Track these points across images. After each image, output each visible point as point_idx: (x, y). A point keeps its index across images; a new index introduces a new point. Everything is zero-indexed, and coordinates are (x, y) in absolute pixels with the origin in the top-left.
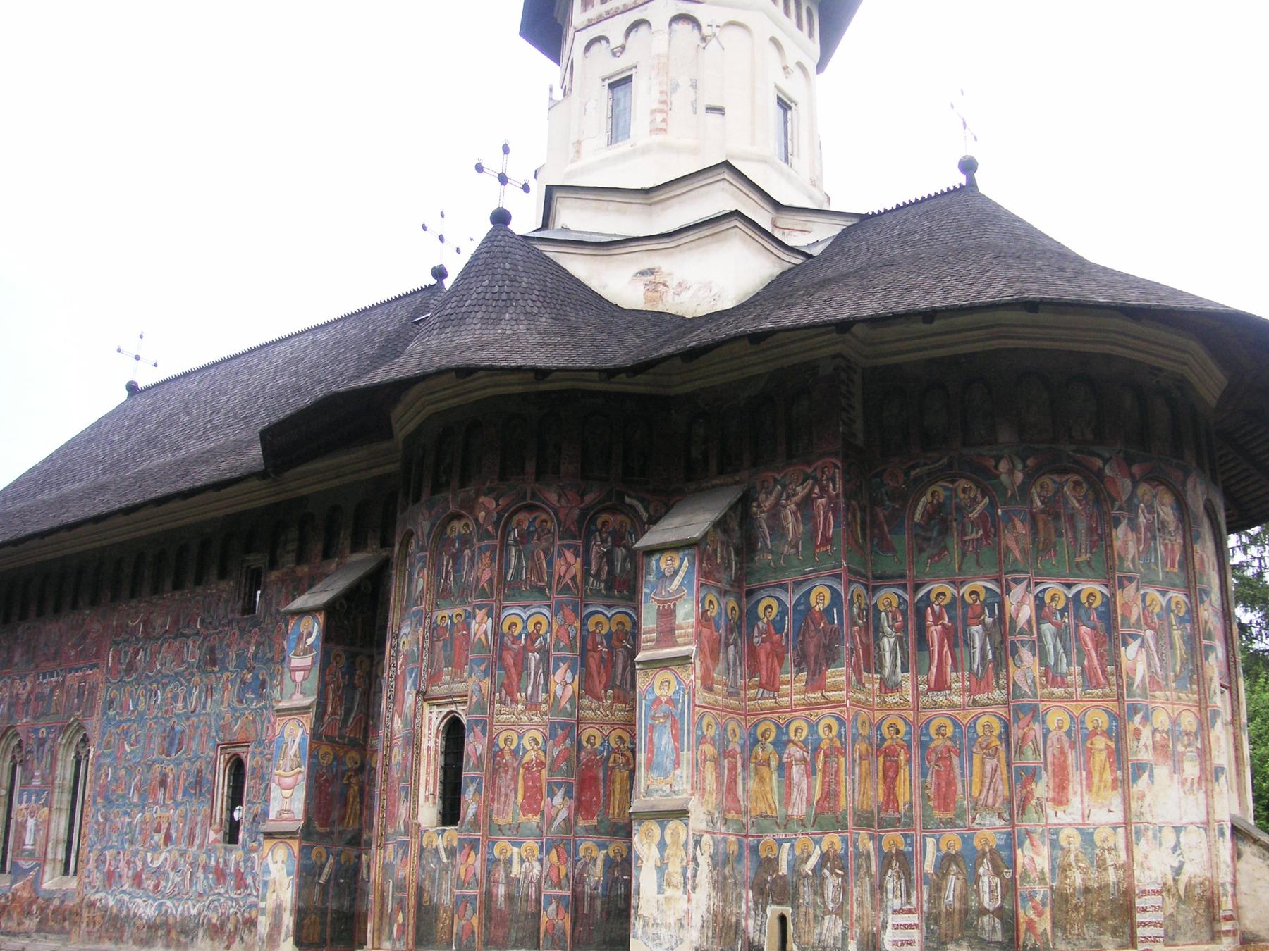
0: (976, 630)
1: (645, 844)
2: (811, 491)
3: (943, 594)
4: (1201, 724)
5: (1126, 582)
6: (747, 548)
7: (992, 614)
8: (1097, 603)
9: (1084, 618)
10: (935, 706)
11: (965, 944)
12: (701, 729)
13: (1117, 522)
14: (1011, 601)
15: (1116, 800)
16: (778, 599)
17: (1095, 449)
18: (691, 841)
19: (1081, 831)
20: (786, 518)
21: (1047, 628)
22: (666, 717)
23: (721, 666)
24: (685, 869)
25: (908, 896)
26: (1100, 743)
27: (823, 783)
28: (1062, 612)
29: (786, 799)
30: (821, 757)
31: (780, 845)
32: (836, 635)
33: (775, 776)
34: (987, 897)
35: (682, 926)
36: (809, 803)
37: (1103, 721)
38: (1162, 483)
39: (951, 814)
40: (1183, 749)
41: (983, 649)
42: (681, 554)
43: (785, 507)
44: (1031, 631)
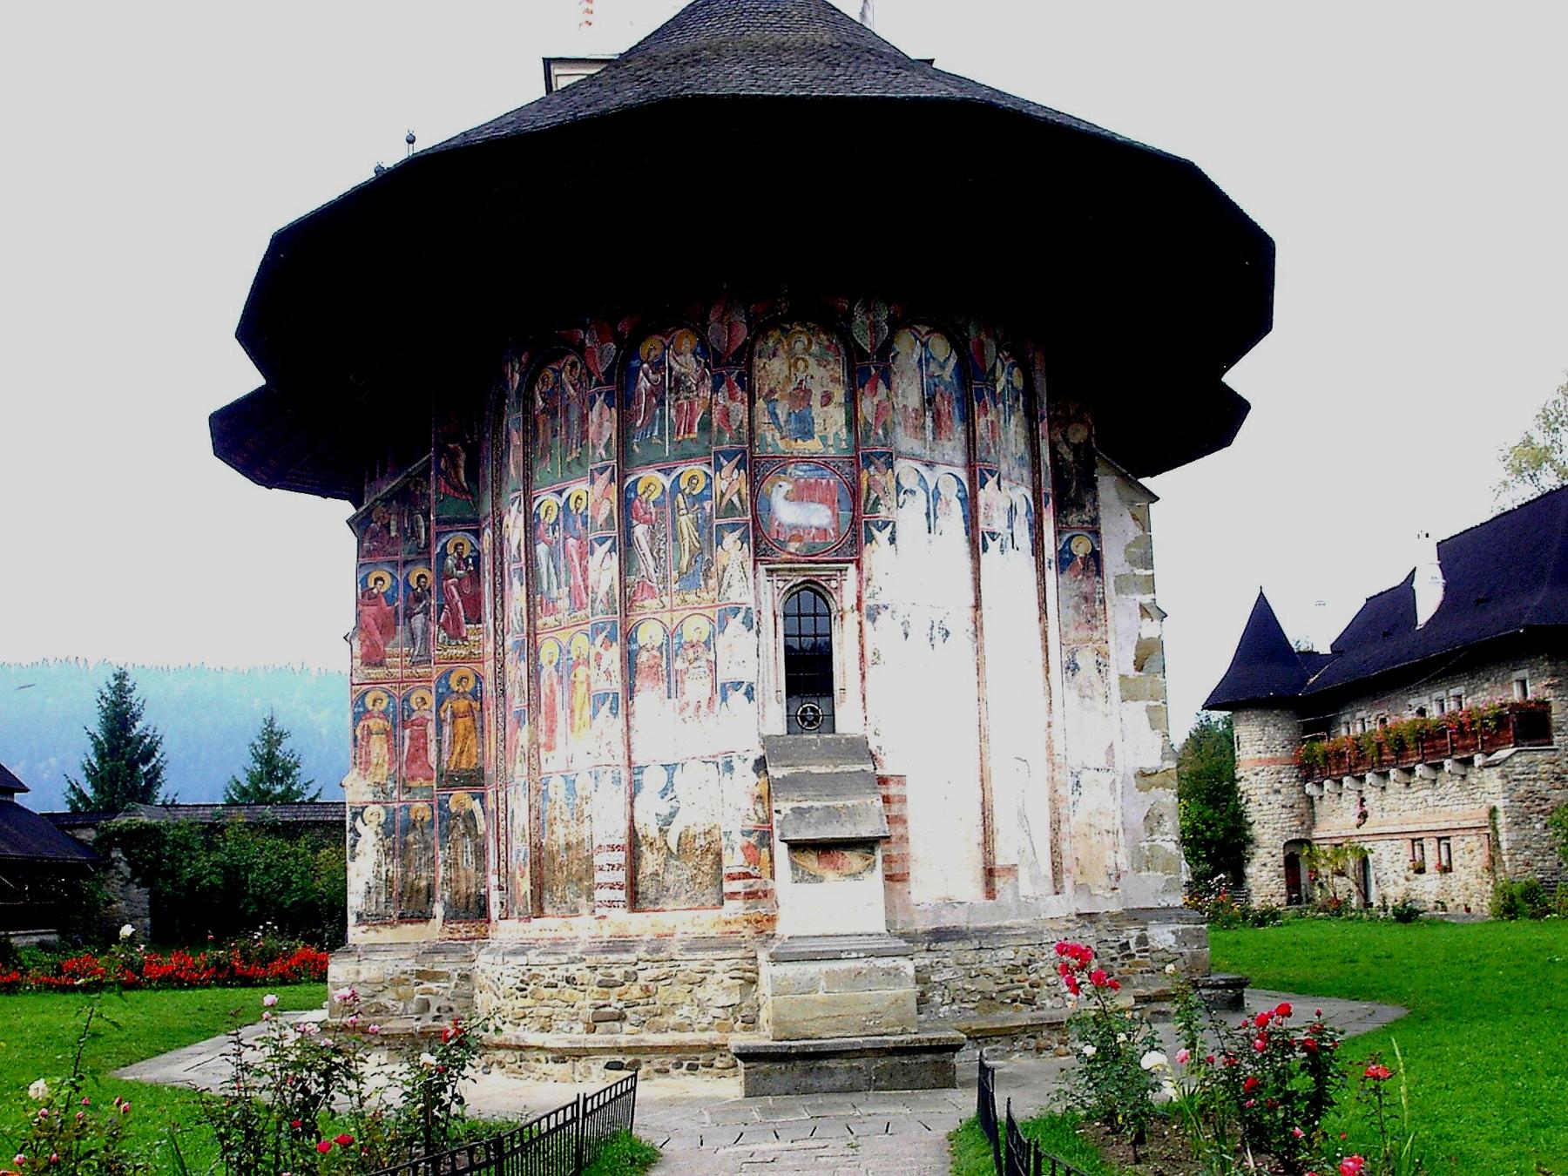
12: (363, 703)
13: (593, 401)
23: (401, 634)
26: (581, 671)
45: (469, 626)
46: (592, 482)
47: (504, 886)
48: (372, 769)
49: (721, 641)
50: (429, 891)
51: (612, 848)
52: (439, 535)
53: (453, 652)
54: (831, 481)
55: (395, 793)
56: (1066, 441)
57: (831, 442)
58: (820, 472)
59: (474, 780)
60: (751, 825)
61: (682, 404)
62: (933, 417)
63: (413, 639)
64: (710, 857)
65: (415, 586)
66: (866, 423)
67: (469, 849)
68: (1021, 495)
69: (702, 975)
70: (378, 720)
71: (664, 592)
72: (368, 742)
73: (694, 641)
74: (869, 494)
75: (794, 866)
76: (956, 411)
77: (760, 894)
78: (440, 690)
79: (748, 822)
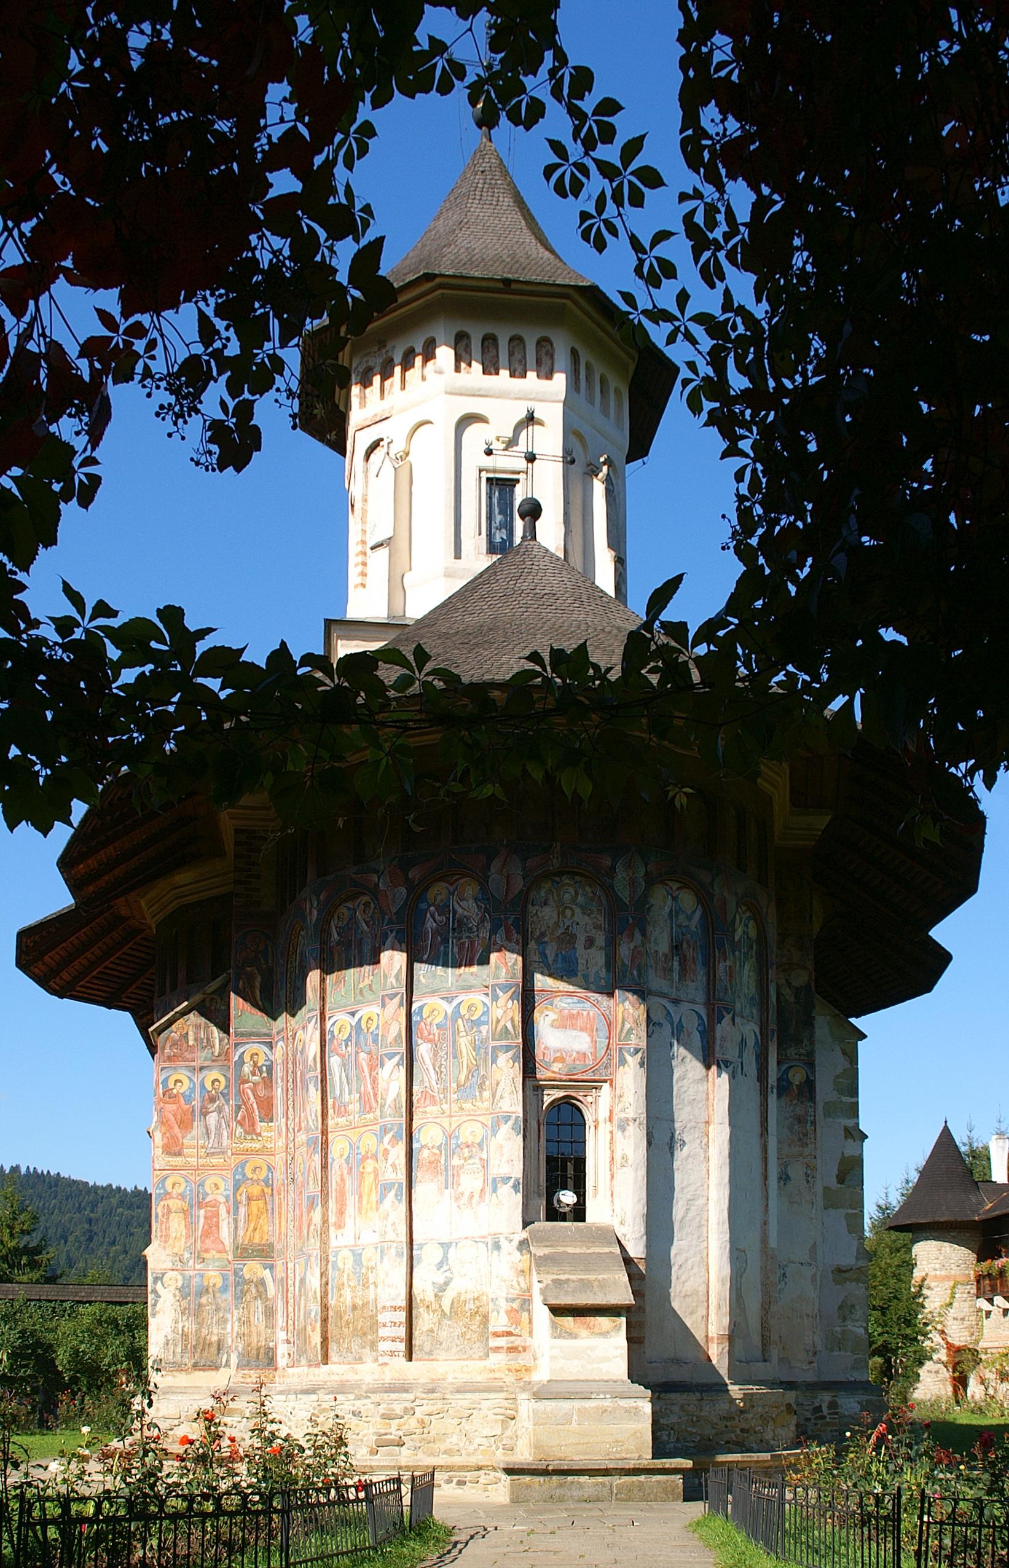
5: (387, 1000)
9: (363, 1044)
12: (163, 1185)
23: (197, 1128)
26: (370, 1165)
28: (346, 1041)
38: (463, 876)
40: (462, 1162)
44: (315, 1067)
45: (262, 1124)
46: (383, 1005)
47: (292, 1340)
48: (171, 1241)
49: (493, 1143)
50: (219, 1345)
51: (395, 1309)
52: (237, 1045)
53: (248, 1145)
54: (591, 1013)
55: (191, 1263)
56: (789, 984)
57: (592, 979)
58: (581, 1005)
59: (264, 1253)
60: (514, 1293)
61: (464, 943)
62: (680, 961)
63: (208, 1134)
64: (478, 1318)
65: (210, 1089)
66: (623, 964)
67: (260, 1309)
68: (750, 1029)
69: (470, 1412)
70: (177, 1201)
71: (444, 1100)
72: (168, 1219)
73: (470, 1142)
74: (623, 1023)
75: (554, 1326)
76: (700, 956)
77: (520, 1349)
78: (237, 1177)
79: (511, 1291)
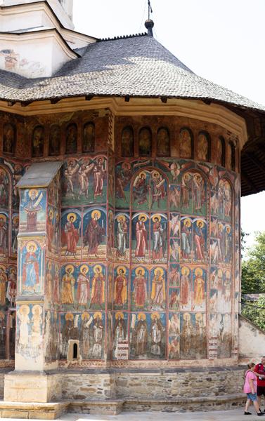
0: (157, 233)
1: (22, 314)
2: (93, 168)
3: (144, 217)
4: (232, 276)
6: (63, 190)
7: (163, 227)
8: (202, 226)
10: (138, 262)
11: (146, 355)
14: (172, 223)
15: (204, 303)
16: (76, 214)
17: (207, 163)
18: (44, 314)
19: (191, 314)
20: (81, 179)
21: (184, 235)
22: (32, 261)
24: (41, 325)
25: (125, 336)
26: (200, 281)
27: (95, 290)
29: (78, 297)
30: (94, 281)
31: (75, 315)
32: (102, 231)
33: (73, 288)
34: (155, 338)
35: (40, 348)
36: (88, 299)
37: (201, 273)
39: (142, 305)
41: (159, 241)
42: (39, 191)
43: (80, 174)
51: (216, 338)
